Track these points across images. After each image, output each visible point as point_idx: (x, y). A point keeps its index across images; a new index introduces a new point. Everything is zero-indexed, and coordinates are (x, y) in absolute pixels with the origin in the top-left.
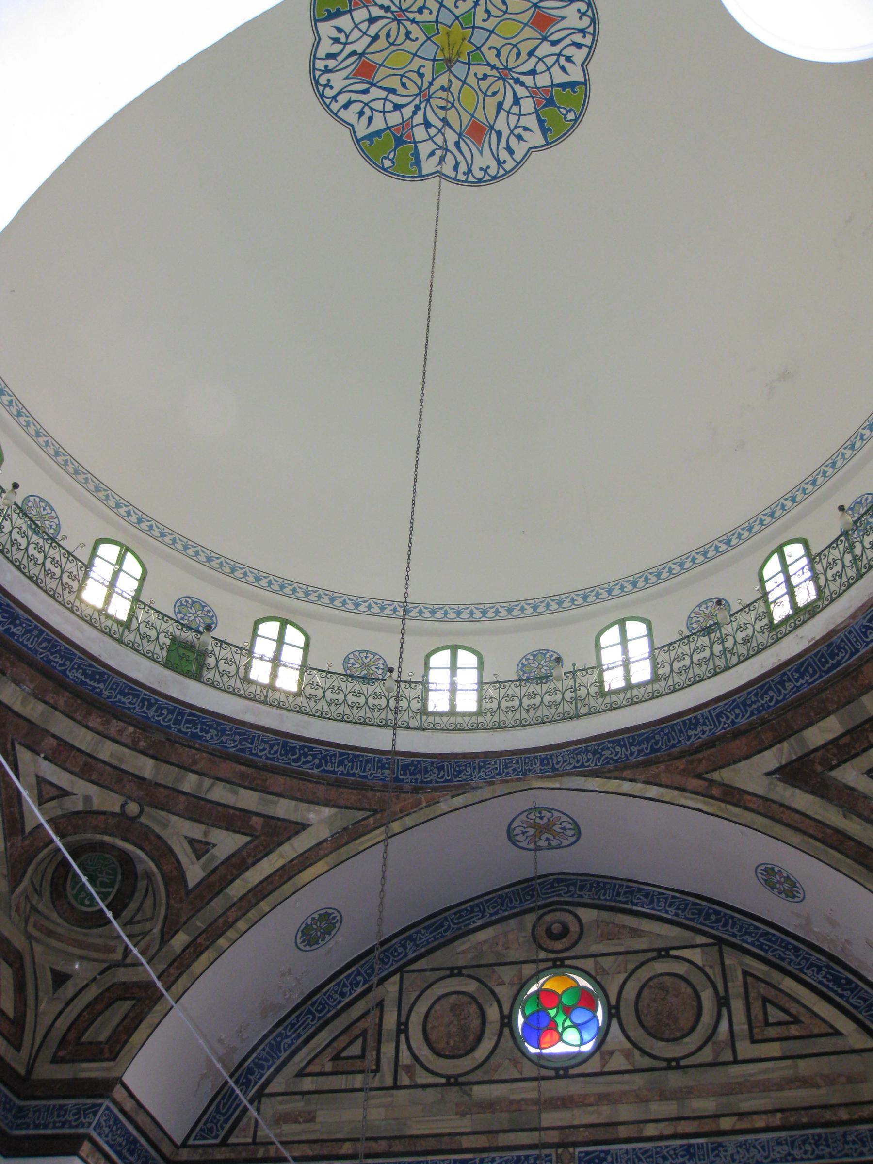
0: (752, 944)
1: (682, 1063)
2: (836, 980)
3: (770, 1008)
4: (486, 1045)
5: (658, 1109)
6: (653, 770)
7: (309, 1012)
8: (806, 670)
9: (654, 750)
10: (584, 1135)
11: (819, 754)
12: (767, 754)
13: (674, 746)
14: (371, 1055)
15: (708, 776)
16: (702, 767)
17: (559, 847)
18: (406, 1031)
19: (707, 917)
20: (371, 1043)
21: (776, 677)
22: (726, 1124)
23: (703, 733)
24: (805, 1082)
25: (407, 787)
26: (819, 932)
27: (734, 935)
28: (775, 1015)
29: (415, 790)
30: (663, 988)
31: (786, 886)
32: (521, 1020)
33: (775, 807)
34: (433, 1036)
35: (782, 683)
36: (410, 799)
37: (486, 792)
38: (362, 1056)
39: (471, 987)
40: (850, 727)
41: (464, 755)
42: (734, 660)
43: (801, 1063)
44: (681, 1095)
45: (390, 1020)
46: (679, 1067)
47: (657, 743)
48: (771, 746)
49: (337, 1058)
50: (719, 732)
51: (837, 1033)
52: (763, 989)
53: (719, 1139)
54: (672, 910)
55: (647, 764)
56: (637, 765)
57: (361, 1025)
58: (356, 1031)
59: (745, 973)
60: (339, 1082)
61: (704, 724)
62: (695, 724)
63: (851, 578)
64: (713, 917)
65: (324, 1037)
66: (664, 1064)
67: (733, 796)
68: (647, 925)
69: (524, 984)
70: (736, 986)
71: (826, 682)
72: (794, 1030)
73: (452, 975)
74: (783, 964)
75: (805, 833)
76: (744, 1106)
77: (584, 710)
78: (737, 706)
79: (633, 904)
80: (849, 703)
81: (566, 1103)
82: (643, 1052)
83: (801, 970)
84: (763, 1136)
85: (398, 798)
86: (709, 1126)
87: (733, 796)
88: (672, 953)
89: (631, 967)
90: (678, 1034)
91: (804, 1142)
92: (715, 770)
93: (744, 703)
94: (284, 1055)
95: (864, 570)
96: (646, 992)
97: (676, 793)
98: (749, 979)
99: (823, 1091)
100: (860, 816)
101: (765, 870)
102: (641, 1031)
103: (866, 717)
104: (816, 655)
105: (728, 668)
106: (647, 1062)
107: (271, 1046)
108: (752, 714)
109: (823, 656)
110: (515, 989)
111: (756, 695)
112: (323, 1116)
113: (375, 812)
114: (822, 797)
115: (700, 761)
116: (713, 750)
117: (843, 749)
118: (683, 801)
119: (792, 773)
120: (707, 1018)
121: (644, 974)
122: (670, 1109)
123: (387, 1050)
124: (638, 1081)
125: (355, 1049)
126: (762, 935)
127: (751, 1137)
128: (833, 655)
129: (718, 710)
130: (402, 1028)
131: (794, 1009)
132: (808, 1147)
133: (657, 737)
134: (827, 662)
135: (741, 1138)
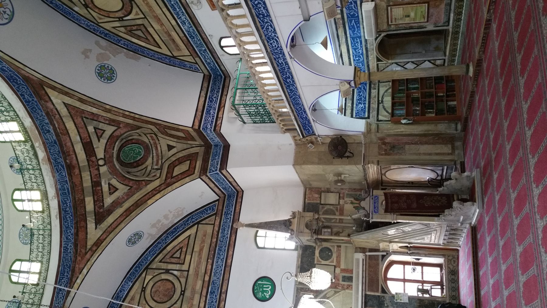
0: (151, 257)
1: (183, 290)
2: (173, 232)
3: (174, 256)
6: (77, 270)
8: (65, 201)
11: (96, 208)
12: (88, 226)
13: (71, 259)
15: (87, 250)
19: (136, 271)
21: (63, 212)
22: (207, 278)
23: (71, 246)
24: (201, 250)
26: (156, 233)
27: (146, 263)
28: (177, 254)
30: (156, 292)
31: (137, 237)
33: (109, 229)
35: (66, 211)
40: (92, 194)
42: (49, 227)
43: (195, 250)
44: (193, 292)
46: (184, 291)
47: (67, 265)
48: (87, 224)
50: (73, 241)
51: (189, 236)
52: (168, 257)
53: (211, 281)
55: (73, 271)
56: (72, 275)
59: (160, 262)
61: (68, 245)
62: (66, 249)
63: (39, 173)
64: (137, 269)
66: (182, 296)
67: (99, 243)
68: (132, 293)
70: (164, 266)
71: (72, 195)
72: (184, 250)
74: (162, 248)
75: (122, 221)
76: (203, 271)
78: (67, 231)
79: (122, 297)
80: (83, 191)
83: (166, 243)
84: (214, 267)
86: (206, 285)
87: (99, 243)
88: (144, 286)
89: (144, 302)
90: (173, 289)
91: (219, 254)
92: (86, 247)
93: (66, 228)
95: (39, 167)
96: (155, 298)
97: (89, 263)
98: (163, 261)
99: (206, 245)
100: (124, 202)
101: (129, 242)
102: (167, 303)
103: (91, 188)
104: (61, 195)
105: (51, 230)
106: (179, 303)
108: (72, 227)
109: (63, 193)
111: (66, 222)
114: (111, 213)
115: (81, 251)
116: (79, 245)
117: (98, 199)
118: (93, 261)
119: (99, 219)
120: (171, 278)
122: (197, 297)
126: (150, 253)
128: (64, 190)
129: (65, 238)
131: (178, 248)
132: (221, 253)
133: (65, 264)
134: (65, 193)
135: (213, 274)
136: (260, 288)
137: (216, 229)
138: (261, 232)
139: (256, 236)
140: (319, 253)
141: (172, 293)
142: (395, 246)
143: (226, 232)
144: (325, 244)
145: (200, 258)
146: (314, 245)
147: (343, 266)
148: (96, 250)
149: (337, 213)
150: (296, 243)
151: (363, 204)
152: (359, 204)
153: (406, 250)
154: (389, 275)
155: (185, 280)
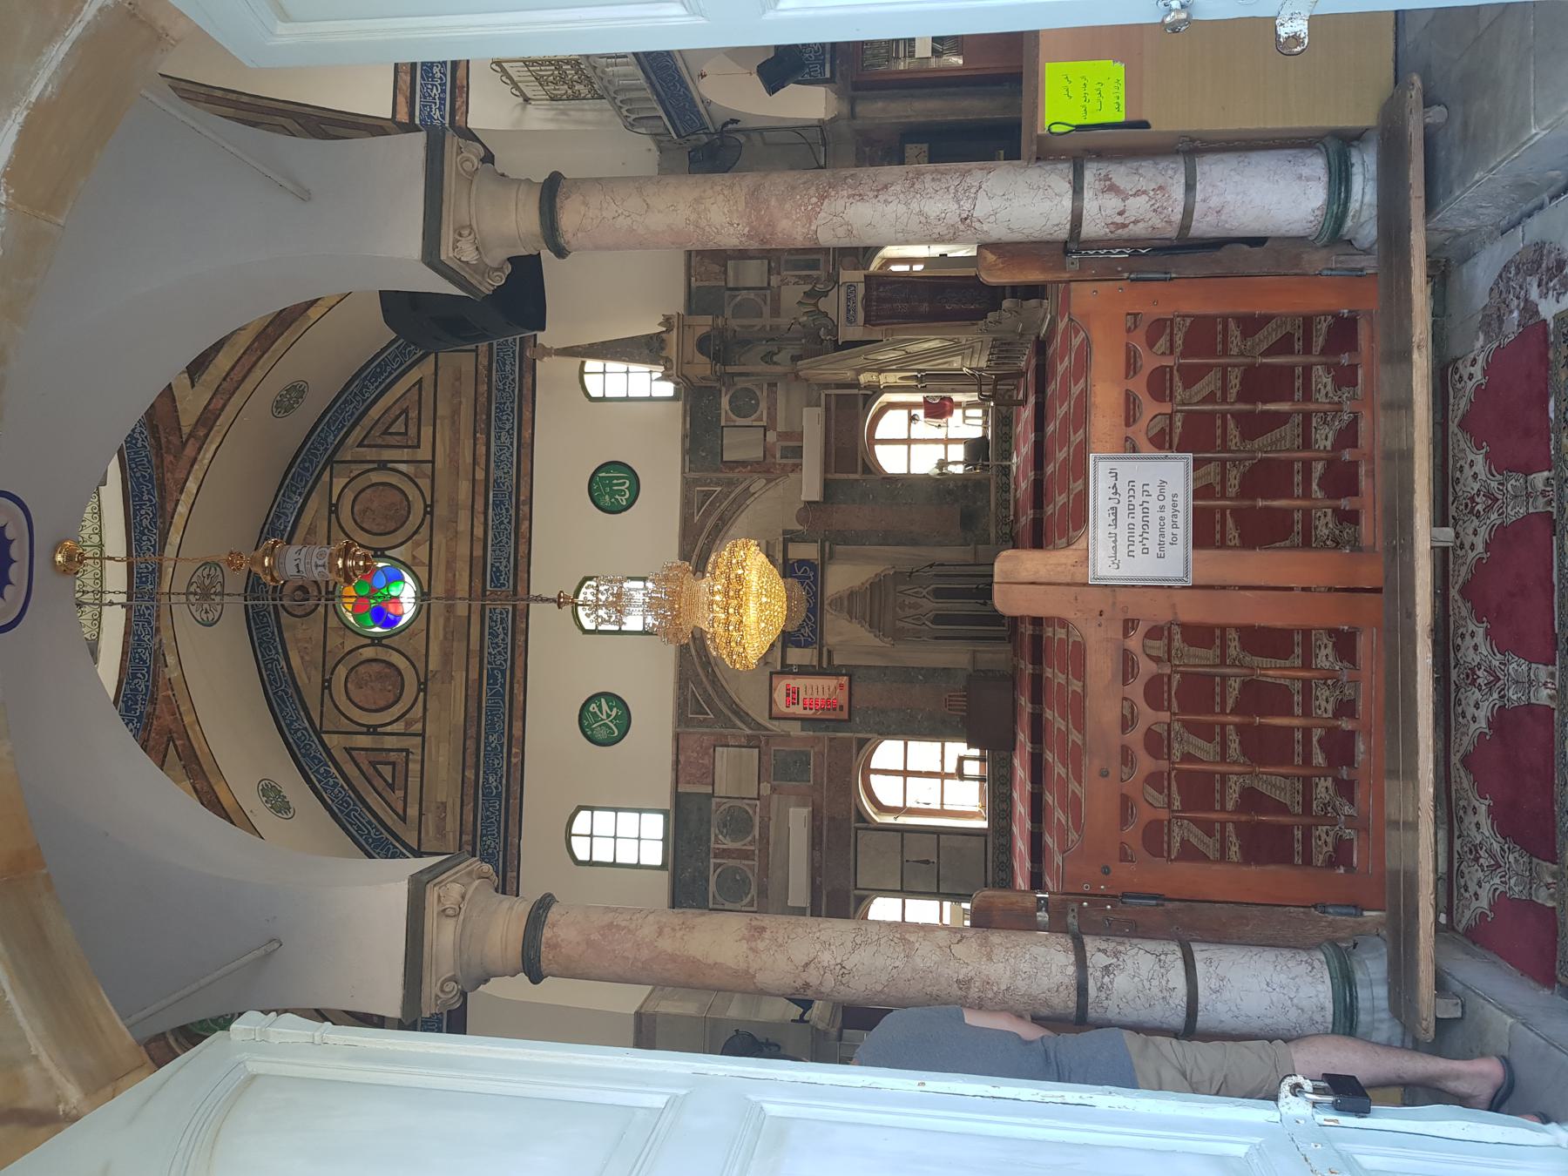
2: (375, 375)
4: (396, 659)
5: (463, 526)
6: (170, 484)
7: (348, 815)
9: (151, 480)
10: (477, 583)
14: (393, 756)
16: (175, 440)
17: (223, 586)
18: (375, 727)
20: (383, 756)
22: (480, 475)
24: (456, 412)
25: (149, 709)
28: (399, 427)
29: (153, 701)
30: (365, 512)
32: (377, 629)
34: (382, 703)
36: (161, 707)
37: (165, 635)
38: (393, 764)
39: (342, 671)
41: (124, 653)
45: (364, 741)
46: (432, 506)
49: (392, 787)
52: (376, 432)
54: (296, 498)
55: (162, 488)
57: (365, 766)
58: (370, 771)
60: (414, 782)
65: (373, 800)
67: (208, 419)
68: (306, 520)
69: (346, 626)
72: (413, 414)
73: (329, 688)
76: (469, 460)
77: (96, 539)
81: (450, 595)
82: (415, 533)
85: (158, 718)
86: (480, 489)
87: (208, 419)
94: (386, 834)
106: (425, 530)
107: (376, 847)
110: (348, 632)
112: (441, 797)
113: (171, 739)
115: (168, 441)
118: (206, 462)
120: (393, 479)
121: (348, 524)
122: (464, 515)
123: (390, 742)
124: (438, 538)
125: (387, 771)
127: (492, 458)
130: (372, 730)
135: (492, 465)
136: (605, 486)
137: (484, 361)
138: (592, 365)
139: (582, 372)
140: (730, 402)
141: (404, 513)
142: (892, 378)
143: (508, 368)
144: (742, 383)
145: (456, 431)
146: (717, 385)
147: (781, 427)
148: (207, 436)
149: (766, 310)
150: (676, 383)
151: (823, 304)
152: (816, 305)
153: (914, 383)
154: (878, 436)
155: (428, 481)
